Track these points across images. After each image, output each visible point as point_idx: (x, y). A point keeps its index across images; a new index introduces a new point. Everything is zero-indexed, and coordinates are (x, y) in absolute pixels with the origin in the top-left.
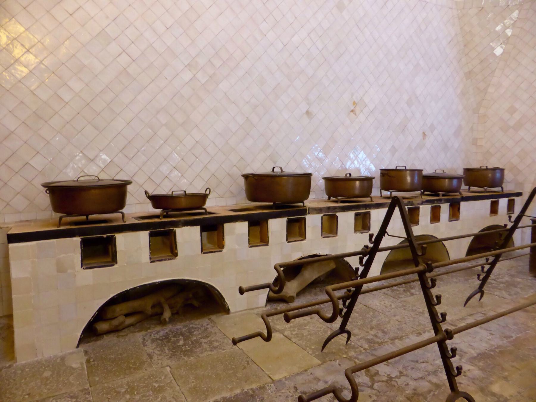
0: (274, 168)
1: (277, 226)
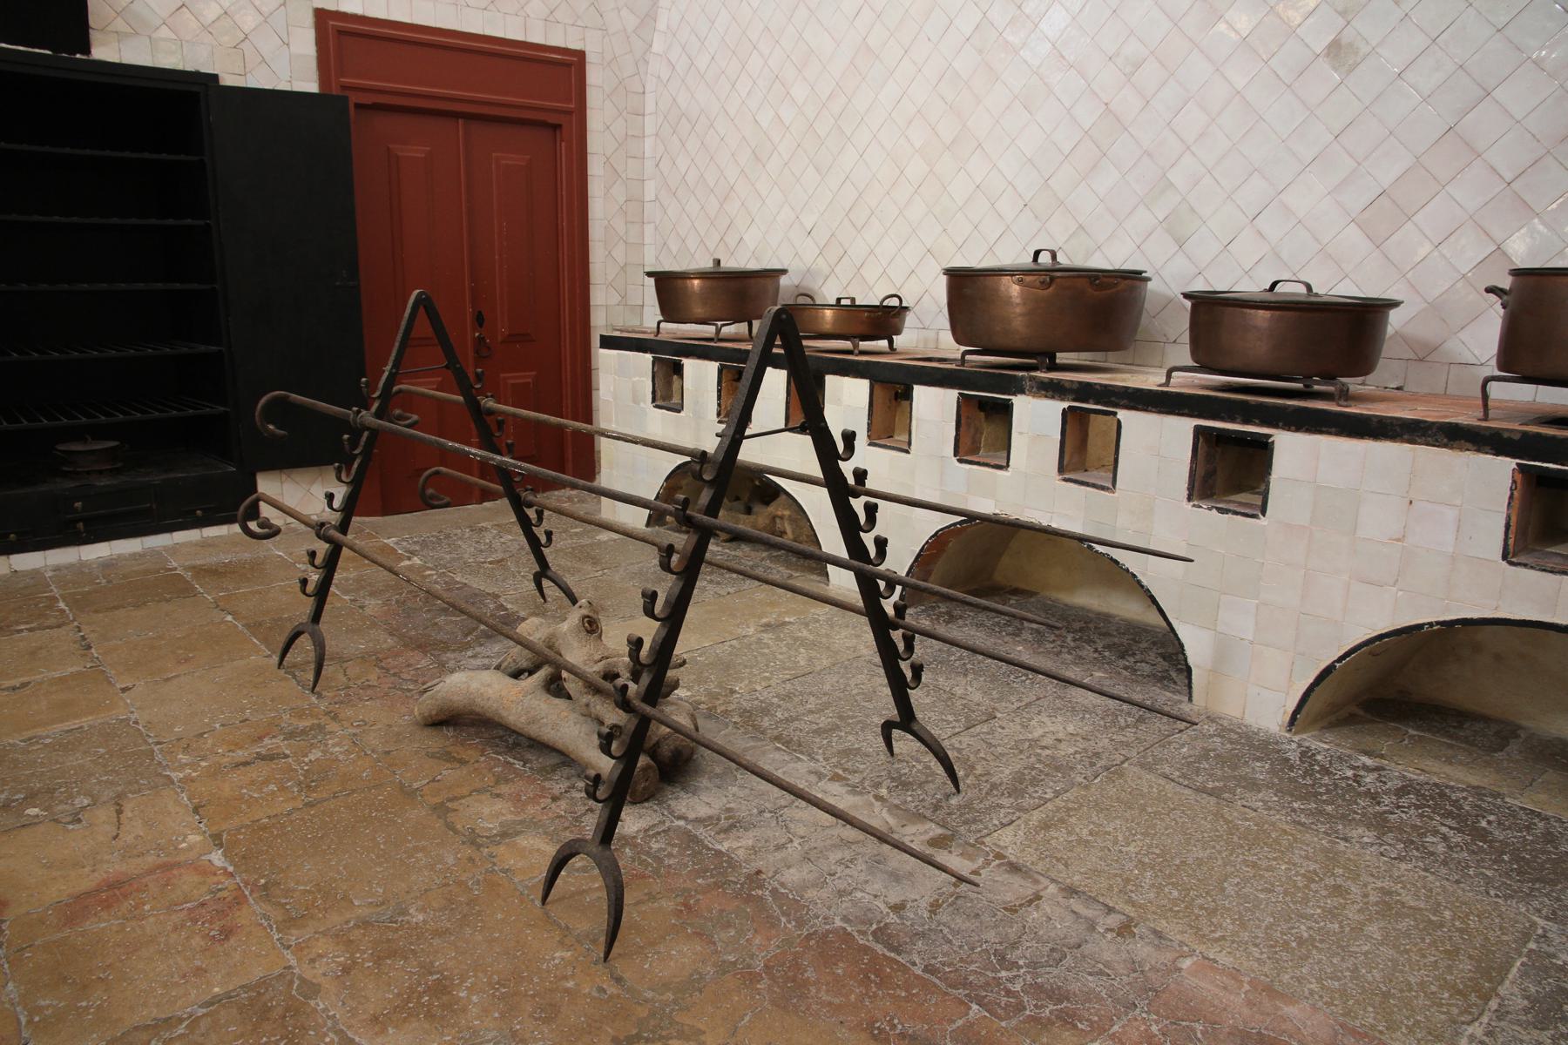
0: (1037, 253)
1: (934, 407)
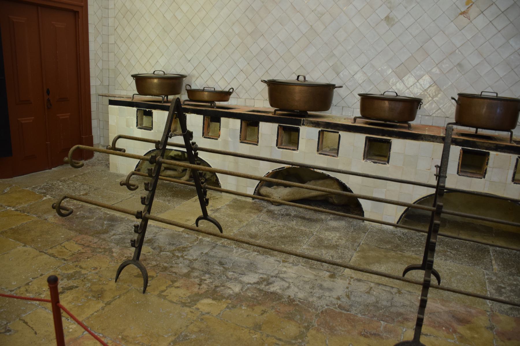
0: (298, 77)
1: (268, 131)
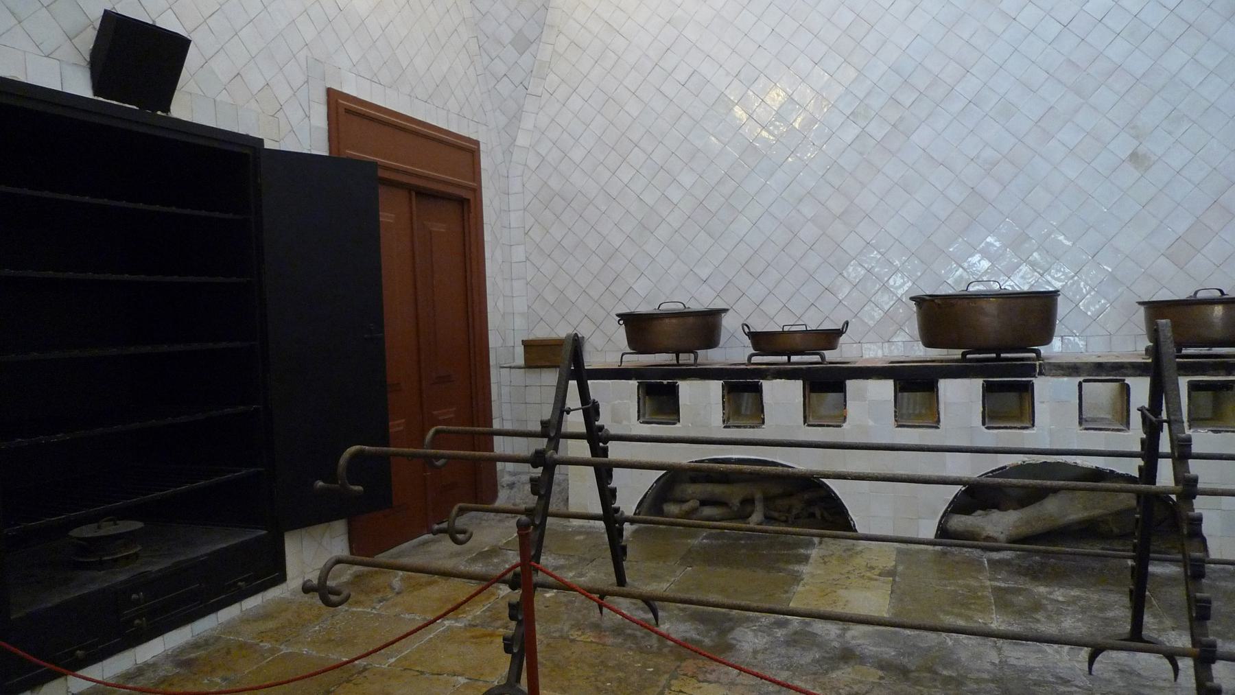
1: (961, 397)
